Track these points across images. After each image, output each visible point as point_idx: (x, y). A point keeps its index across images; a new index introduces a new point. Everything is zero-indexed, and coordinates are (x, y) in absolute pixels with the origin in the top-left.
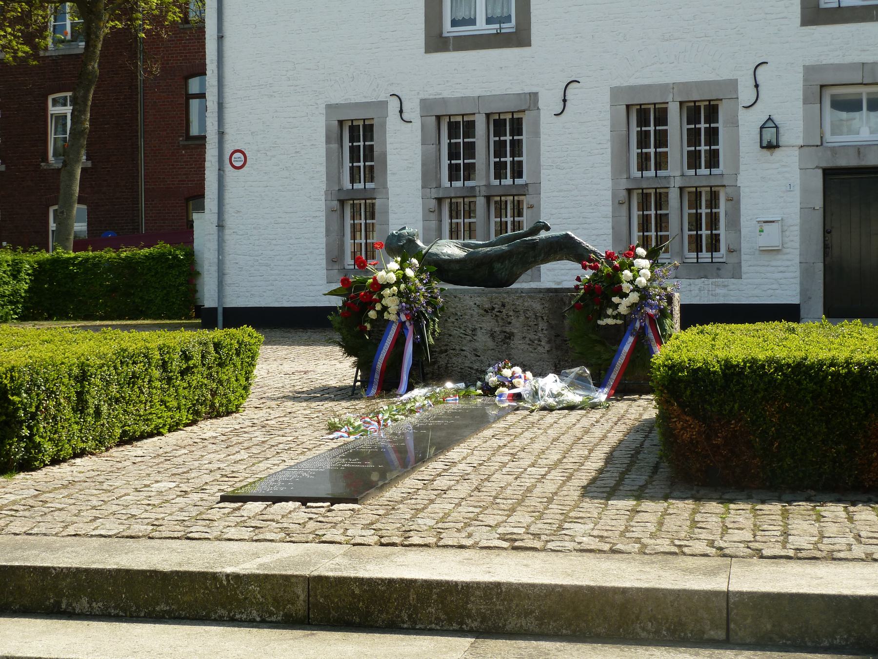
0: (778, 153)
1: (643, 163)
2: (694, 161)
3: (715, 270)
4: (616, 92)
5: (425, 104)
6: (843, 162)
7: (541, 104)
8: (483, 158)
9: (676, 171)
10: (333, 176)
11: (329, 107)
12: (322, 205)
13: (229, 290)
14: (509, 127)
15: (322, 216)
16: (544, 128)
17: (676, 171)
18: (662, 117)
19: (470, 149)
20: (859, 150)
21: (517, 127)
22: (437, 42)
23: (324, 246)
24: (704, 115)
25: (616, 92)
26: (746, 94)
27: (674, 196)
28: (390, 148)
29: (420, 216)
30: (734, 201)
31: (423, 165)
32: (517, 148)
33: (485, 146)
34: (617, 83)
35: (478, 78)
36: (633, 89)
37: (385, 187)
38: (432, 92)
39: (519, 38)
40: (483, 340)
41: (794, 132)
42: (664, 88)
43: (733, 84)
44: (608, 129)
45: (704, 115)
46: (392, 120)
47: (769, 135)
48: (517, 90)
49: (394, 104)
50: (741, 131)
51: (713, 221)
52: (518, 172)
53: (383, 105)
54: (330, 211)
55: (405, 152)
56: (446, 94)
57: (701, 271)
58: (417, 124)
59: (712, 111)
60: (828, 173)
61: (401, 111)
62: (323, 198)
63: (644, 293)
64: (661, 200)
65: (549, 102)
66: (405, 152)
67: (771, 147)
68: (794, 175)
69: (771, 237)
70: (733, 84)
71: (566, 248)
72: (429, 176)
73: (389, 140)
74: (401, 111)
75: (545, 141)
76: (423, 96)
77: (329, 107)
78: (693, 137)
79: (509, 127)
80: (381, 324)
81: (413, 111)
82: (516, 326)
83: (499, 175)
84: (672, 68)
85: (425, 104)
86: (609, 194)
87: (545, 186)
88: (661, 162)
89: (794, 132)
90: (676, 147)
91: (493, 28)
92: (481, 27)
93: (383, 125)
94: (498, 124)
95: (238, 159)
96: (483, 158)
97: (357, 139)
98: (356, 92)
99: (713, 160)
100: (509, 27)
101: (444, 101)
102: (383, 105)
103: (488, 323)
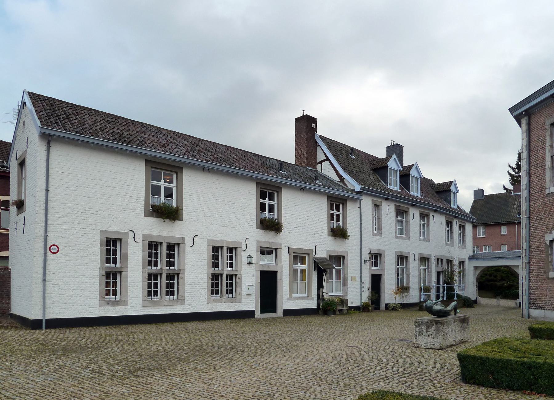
0: (251, 265)
4: (209, 241)
5: (144, 235)
6: (265, 269)
11: (102, 231)
13: (47, 311)
15: (98, 278)
16: (186, 251)
23: (98, 290)
25: (209, 241)
26: (244, 247)
29: (141, 279)
31: (143, 259)
34: (209, 238)
36: (214, 241)
37: (127, 267)
41: (255, 261)
42: (222, 242)
43: (240, 243)
44: (206, 254)
46: (130, 241)
48: (178, 236)
49: (131, 235)
50: (242, 257)
53: (127, 234)
56: (152, 234)
58: (141, 244)
61: (134, 238)
62: (98, 270)
67: (250, 263)
68: (254, 272)
70: (240, 243)
73: (129, 249)
74: (134, 238)
75: (187, 256)
76: (144, 233)
77: (102, 231)
81: (139, 238)
84: (226, 237)
85: (144, 235)
86: (206, 275)
87: (187, 271)
93: (127, 242)
95: (54, 249)
97: (112, 245)
98: (115, 227)
101: (151, 236)
102: (127, 234)
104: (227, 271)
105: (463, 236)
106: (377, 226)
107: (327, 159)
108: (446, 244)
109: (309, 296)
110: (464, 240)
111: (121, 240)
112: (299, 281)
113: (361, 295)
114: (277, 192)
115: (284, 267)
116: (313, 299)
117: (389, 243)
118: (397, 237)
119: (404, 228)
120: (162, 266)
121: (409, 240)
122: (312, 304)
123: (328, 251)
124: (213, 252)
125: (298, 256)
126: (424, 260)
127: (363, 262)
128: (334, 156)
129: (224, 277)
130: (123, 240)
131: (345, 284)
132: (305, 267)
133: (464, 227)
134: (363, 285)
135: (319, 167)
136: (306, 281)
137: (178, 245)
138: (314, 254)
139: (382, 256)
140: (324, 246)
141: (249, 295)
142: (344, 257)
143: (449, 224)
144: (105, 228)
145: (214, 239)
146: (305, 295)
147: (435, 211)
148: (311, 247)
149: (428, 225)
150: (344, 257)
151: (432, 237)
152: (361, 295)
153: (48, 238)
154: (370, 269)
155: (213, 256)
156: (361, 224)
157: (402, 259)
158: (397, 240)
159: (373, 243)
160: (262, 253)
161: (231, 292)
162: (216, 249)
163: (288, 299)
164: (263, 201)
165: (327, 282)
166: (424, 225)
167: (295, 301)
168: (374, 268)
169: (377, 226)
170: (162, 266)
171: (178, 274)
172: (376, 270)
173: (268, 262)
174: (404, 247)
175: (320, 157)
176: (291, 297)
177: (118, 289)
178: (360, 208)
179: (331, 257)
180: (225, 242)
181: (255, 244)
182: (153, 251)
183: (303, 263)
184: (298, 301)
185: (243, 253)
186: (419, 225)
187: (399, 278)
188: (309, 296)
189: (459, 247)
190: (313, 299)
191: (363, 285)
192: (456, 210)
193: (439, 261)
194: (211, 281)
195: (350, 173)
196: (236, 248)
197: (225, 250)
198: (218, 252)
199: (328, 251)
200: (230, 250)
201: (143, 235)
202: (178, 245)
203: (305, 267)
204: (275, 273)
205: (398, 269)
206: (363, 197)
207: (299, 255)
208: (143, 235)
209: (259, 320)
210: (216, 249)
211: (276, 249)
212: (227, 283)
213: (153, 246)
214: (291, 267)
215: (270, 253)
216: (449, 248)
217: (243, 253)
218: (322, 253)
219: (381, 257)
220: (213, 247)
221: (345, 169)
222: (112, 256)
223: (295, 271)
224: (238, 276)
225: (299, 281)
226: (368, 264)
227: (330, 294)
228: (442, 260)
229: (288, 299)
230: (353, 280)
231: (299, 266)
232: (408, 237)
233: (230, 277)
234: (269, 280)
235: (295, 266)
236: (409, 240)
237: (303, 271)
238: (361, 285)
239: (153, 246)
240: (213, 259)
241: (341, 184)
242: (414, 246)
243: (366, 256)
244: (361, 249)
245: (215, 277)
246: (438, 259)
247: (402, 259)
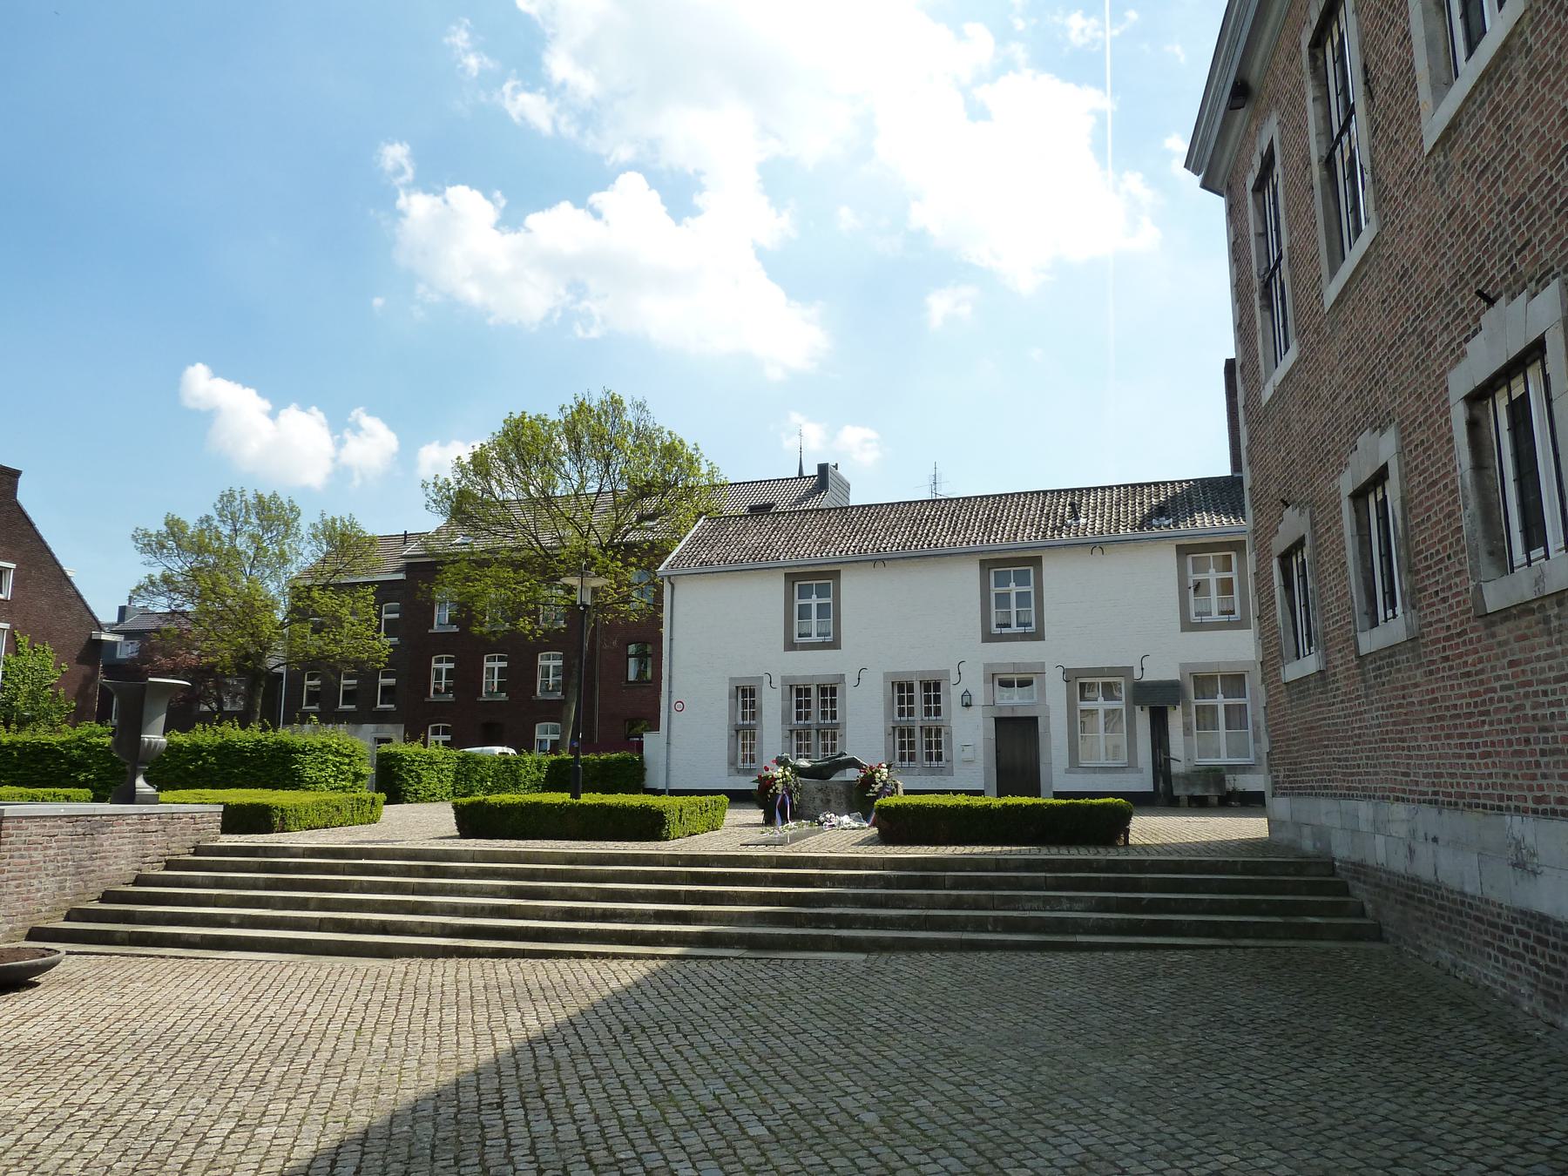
1: (901, 713)
2: (928, 712)
3: (940, 771)
4: (886, 675)
8: (815, 709)
9: (919, 718)
10: (732, 717)
13: (672, 780)
14: (829, 692)
17: (919, 718)
18: (911, 688)
19: (808, 703)
20: (1013, 708)
21: (833, 691)
22: (790, 646)
24: (933, 688)
25: (886, 675)
26: (954, 678)
27: (917, 730)
30: (949, 734)
32: (833, 703)
33: (816, 703)
35: (813, 666)
38: (787, 673)
39: (835, 645)
40: (818, 802)
41: (979, 697)
42: (912, 673)
45: (933, 688)
47: (966, 700)
50: (951, 698)
51: (938, 745)
52: (834, 716)
54: (731, 736)
55: (772, 704)
57: (932, 771)
59: (937, 686)
60: (998, 720)
63: (885, 783)
64: (911, 733)
65: (850, 680)
66: (772, 704)
67: (968, 705)
69: (968, 753)
71: (853, 763)
72: (786, 718)
78: (928, 700)
79: (829, 692)
80: (775, 795)
81: (777, 682)
82: (832, 797)
83: (824, 718)
84: (917, 663)
88: (911, 713)
89: (979, 697)
90: (919, 705)
91: (821, 639)
92: (814, 638)
94: (823, 690)
96: (815, 709)
97: (746, 695)
98: (746, 672)
99: (938, 712)
100: (829, 639)
103: (820, 795)
115: (1052, 705)
116: (1140, 771)
123: (1183, 666)
125: (1081, 683)
138: (1137, 675)
162: (902, 688)
163: (1067, 771)
173: (1015, 701)
176: (1074, 764)
188: (1131, 766)
190: (1140, 771)
199: (1183, 666)
204: (1034, 720)
210: (902, 688)
213: (800, 694)
214: (1071, 706)
218: (1161, 670)
229: (1067, 771)
239: (800, 694)
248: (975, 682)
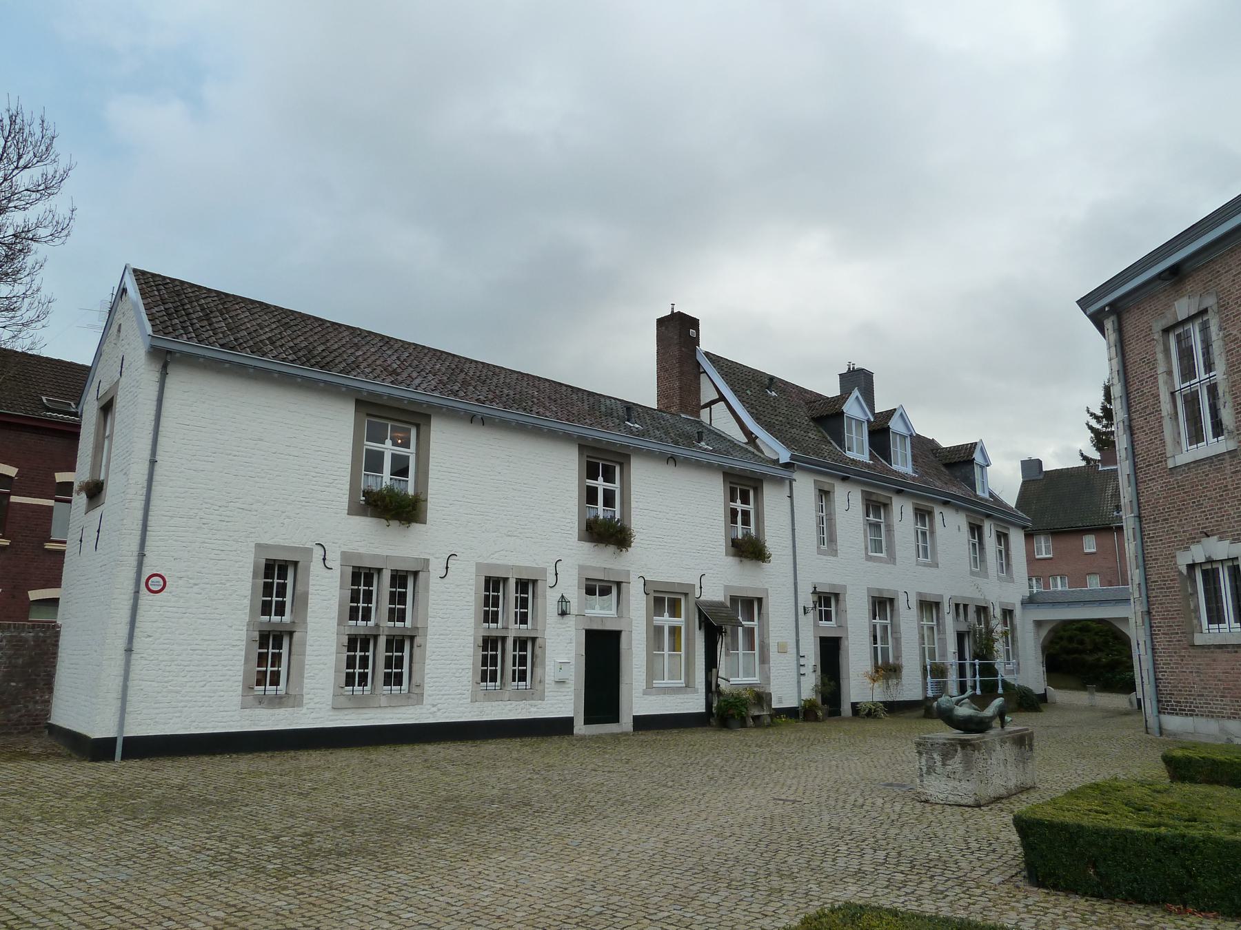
4: (479, 566)
5: (345, 556)
6: (595, 627)
7: (430, 568)
11: (258, 546)
12: (243, 634)
25: (479, 566)
26: (551, 580)
28: (311, 590)
34: (481, 560)
41: (574, 608)
43: (544, 570)
44: (473, 593)
46: (316, 566)
49: (318, 553)
50: (548, 601)
53: (309, 551)
56: (361, 550)
57: (523, 696)
58: (337, 572)
61: (324, 559)
65: (436, 568)
67: (563, 613)
70: (544, 570)
74: (324, 559)
75: (432, 597)
76: (345, 549)
77: (258, 546)
81: (335, 560)
84: (514, 558)
85: (345, 556)
87: (431, 630)
93: (307, 569)
97: (277, 575)
98: (284, 537)
101: (360, 556)
102: (309, 551)
104: (515, 630)
105: (1005, 555)
106: (827, 535)
107: (722, 398)
108: (972, 573)
109: (689, 685)
110: (1008, 564)
111: (296, 564)
112: (666, 652)
113: (799, 682)
114: (621, 465)
115: (634, 621)
116: (696, 691)
117: (854, 572)
118: (869, 558)
119: (883, 538)
120: (380, 619)
121: (894, 563)
122: (695, 703)
124: (487, 589)
125: (665, 599)
126: (929, 606)
127: (801, 611)
128: (735, 392)
129: (510, 644)
130: (300, 565)
131: (764, 660)
132: (679, 621)
133: (1006, 536)
134: (802, 661)
135: (704, 413)
136: (683, 652)
137: (416, 574)
139: (841, 597)
140: (719, 578)
141: (561, 682)
142: (760, 600)
143: (976, 530)
144: (266, 540)
145: (489, 561)
146: (681, 682)
147: (946, 503)
148: (690, 578)
149: (932, 532)
150: (760, 600)
151: (941, 559)
152: (799, 682)
153: (146, 560)
154: (816, 626)
155: (487, 597)
156: (793, 530)
157: (882, 604)
158: (870, 563)
159: (821, 572)
160: (590, 591)
161: (522, 677)
162: (493, 584)
164: (591, 482)
165: (727, 655)
166: (924, 534)
167: (660, 697)
168: (823, 623)
169: (827, 535)
170: (380, 619)
171: (412, 638)
172: (829, 628)
173: (602, 612)
174: (887, 579)
175: (707, 394)
176: (650, 689)
177: (283, 670)
178: (791, 497)
179: (734, 599)
180: (513, 567)
181: (575, 572)
182: (362, 588)
183: (675, 612)
184: (666, 697)
185: (549, 592)
186: (913, 533)
187: (879, 645)
189: (999, 578)
190: (696, 691)
191: (802, 661)
192: (987, 500)
193: (960, 608)
194: (480, 653)
195: (769, 427)
196: (535, 582)
197: (512, 584)
198: (496, 589)
200: (524, 585)
201: (343, 553)
202: (416, 574)
203: (679, 621)
205: (875, 627)
206: (796, 476)
207: (666, 596)
208: (343, 553)
209: (582, 738)
211: (619, 584)
212: (514, 656)
213: (362, 577)
215: (605, 591)
216: (979, 580)
217: (549, 592)
218: (714, 593)
219: (837, 601)
220: (488, 580)
221: (757, 419)
222: (275, 599)
223: (659, 630)
224: (538, 642)
225: (666, 652)
226: (811, 615)
227: (734, 680)
228: (965, 606)
230: (782, 650)
231: (666, 620)
232: (892, 558)
233: (521, 643)
234: (603, 651)
235: (658, 620)
236: (894, 563)
237: (675, 631)
238: (798, 660)
239: (362, 577)
240: (486, 604)
241: (751, 449)
242: (906, 578)
243: (807, 599)
244: (796, 584)
245: (490, 643)
246: (957, 606)
247: (882, 604)
248: (571, 587)
